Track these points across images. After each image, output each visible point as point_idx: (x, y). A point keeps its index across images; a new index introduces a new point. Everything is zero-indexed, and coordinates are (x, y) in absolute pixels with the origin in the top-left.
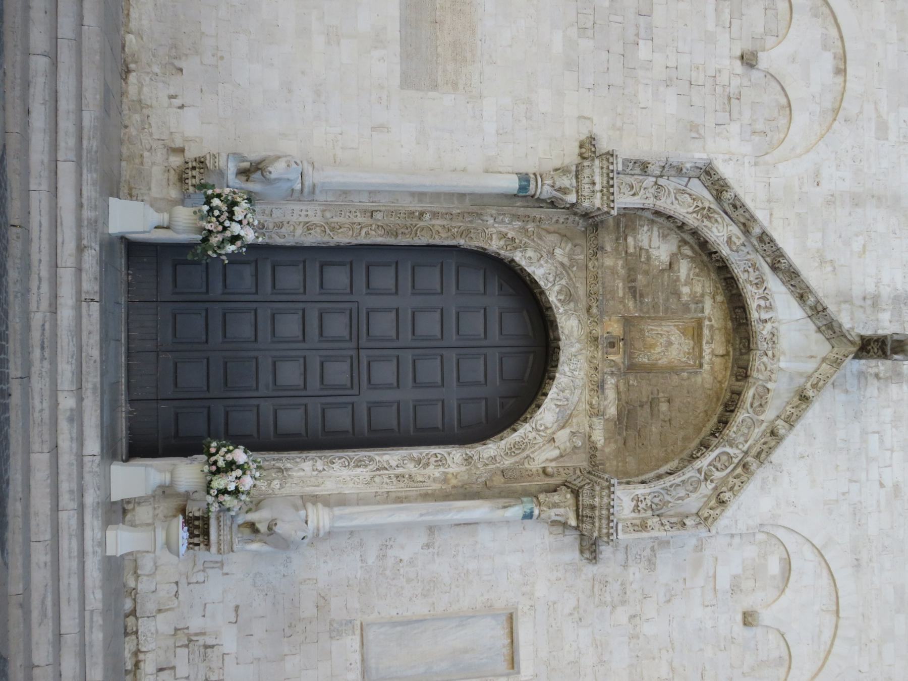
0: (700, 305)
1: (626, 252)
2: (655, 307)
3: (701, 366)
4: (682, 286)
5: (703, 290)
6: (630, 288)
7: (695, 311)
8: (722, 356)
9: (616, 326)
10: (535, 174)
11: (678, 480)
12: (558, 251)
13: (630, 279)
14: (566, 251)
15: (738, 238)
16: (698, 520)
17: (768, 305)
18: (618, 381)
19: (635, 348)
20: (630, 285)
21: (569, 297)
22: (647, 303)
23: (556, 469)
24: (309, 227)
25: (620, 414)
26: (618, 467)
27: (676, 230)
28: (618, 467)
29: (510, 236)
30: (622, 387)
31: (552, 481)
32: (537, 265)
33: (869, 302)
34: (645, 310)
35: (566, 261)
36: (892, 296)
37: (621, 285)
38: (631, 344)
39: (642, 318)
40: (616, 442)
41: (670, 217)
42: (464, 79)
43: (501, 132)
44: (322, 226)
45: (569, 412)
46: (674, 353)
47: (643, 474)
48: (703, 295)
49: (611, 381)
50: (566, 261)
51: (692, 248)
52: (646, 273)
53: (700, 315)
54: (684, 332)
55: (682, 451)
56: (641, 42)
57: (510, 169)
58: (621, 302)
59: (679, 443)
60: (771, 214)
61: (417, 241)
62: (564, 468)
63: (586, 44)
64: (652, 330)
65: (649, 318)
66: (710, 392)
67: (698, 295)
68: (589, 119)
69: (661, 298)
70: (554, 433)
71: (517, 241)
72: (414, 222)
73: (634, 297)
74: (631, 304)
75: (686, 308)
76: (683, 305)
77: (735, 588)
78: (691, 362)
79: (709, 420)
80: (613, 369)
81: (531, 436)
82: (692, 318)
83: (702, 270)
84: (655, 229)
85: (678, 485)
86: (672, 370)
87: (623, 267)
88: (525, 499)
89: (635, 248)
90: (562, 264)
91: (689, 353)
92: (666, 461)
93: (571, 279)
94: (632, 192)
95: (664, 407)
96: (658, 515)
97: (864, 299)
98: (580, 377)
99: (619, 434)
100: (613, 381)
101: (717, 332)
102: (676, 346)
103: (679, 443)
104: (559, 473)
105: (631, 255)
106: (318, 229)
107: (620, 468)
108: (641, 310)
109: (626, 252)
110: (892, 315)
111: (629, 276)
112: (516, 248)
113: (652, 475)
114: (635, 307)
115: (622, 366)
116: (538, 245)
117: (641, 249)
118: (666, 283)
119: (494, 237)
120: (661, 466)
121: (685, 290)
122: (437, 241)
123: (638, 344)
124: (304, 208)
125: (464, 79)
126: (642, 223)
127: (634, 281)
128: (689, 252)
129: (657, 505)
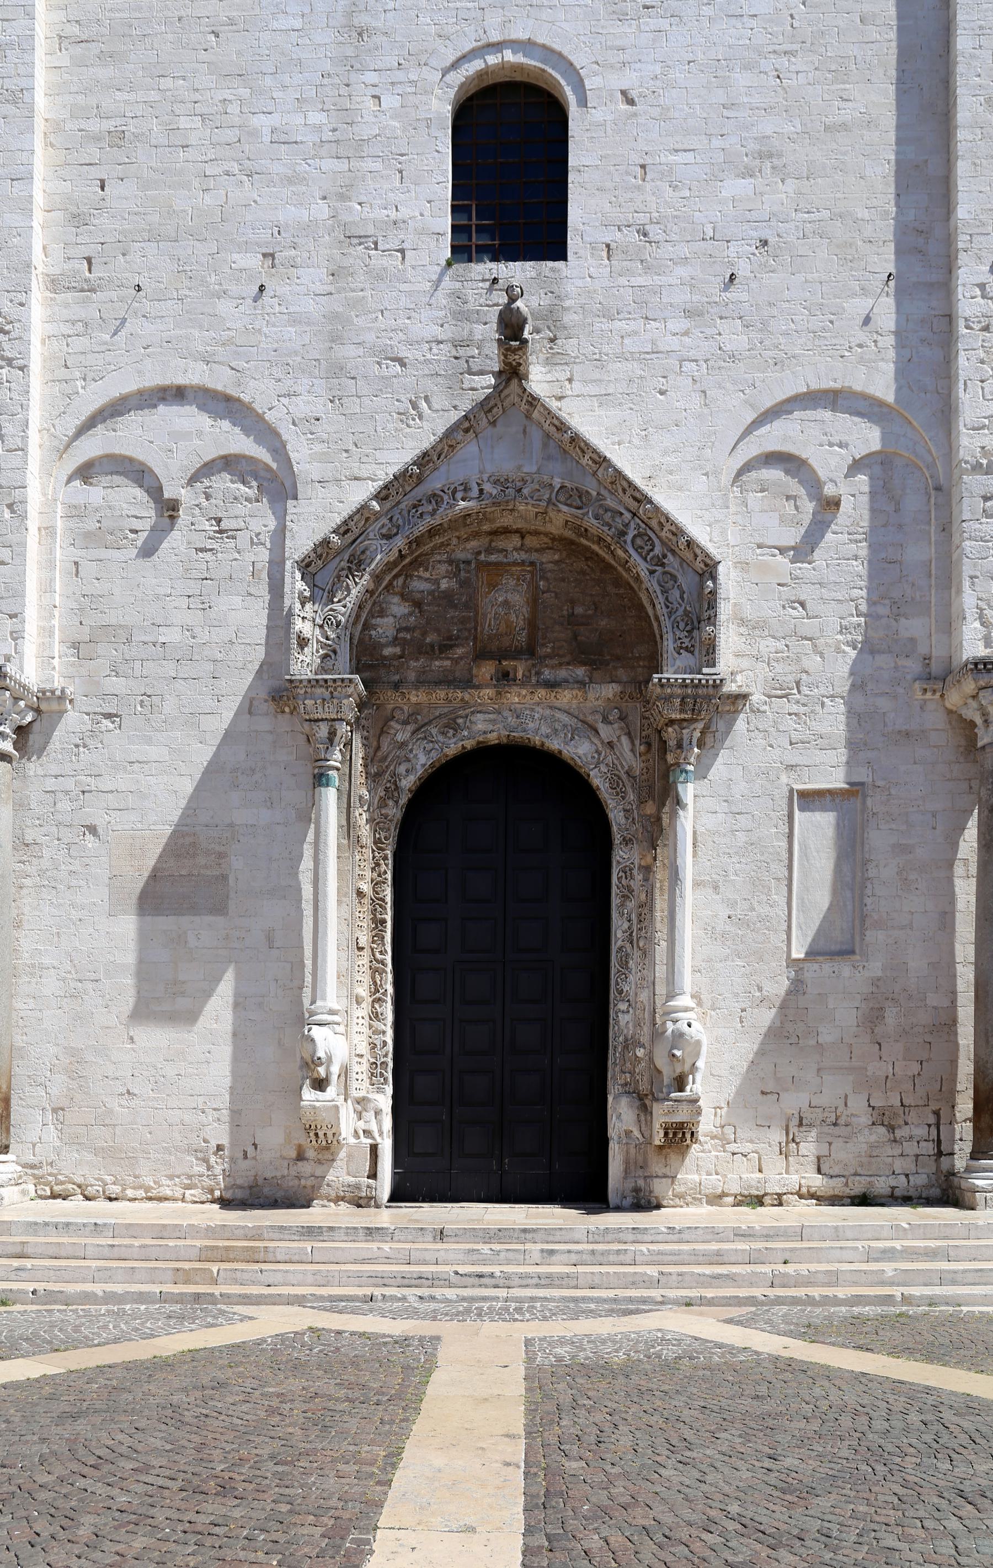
0: (462, 566)
1: (401, 657)
2: (463, 621)
3: (532, 564)
4: (439, 588)
5: (445, 562)
6: (441, 653)
7: (469, 572)
8: (523, 537)
9: (484, 670)
10: (314, 768)
11: (661, 599)
12: (400, 737)
13: (431, 651)
14: (399, 727)
15: (383, 526)
16: (707, 575)
17: (462, 488)
18: (547, 666)
19: (511, 646)
20: (437, 652)
21: (452, 725)
22: (458, 631)
23: (643, 740)
24: (376, 1016)
25: (583, 663)
26: (644, 667)
27: (375, 597)
28: (644, 667)
29: (383, 794)
30: (555, 661)
31: (655, 745)
32: (414, 761)
33: (461, 352)
34: (467, 634)
35: (410, 728)
36: (454, 323)
37: (437, 663)
38: (506, 650)
39: (475, 638)
40: (615, 668)
41: (360, 607)
42: (213, 846)
43: (269, 804)
44: (373, 1001)
45: (580, 725)
46: (517, 597)
47: (655, 636)
48: (450, 562)
49: (547, 674)
50: (410, 728)
51: (396, 577)
52: (424, 634)
53: (473, 566)
54: (493, 586)
55: (631, 588)
56: (162, 639)
57: (310, 793)
58: (457, 663)
59: (622, 591)
60: (356, 479)
61: (389, 899)
62: (642, 730)
63: (169, 706)
64: (489, 625)
65: (476, 629)
66: (564, 553)
67: (450, 568)
68: (251, 702)
69: (452, 614)
70: (602, 743)
71: (388, 785)
72: (366, 901)
73: (451, 647)
74: (460, 651)
75: (464, 583)
76: (461, 587)
77: (795, 521)
78: (528, 576)
79: (597, 555)
80: (533, 672)
81: (604, 769)
82: (477, 576)
83: (421, 565)
84: (373, 621)
85: (667, 599)
86: (534, 601)
87: (417, 660)
88: (671, 779)
89: (396, 646)
90: (413, 733)
91: (518, 579)
92: (641, 607)
93: (430, 722)
94: (333, 657)
95: (579, 610)
96: (699, 623)
97: (456, 358)
98: (541, 710)
99: (608, 664)
100: (547, 672)
101: (494, 544)
102: (509, 596)
103: (622, 591)
104: (648, 736)
105: (403, 650)
106: (377, 1006)
107: (646, 663)
108: (467, 639)
109: (401, 657)
110: (477, 322)
111: (427, 653)
112: (397, 788)
113: (655, 625)
114: (463, 646)
115: (530, 662)
116: (392, 761)
117: (396, 638)
118: (436, 609)
119: (383, 812)
120: (647, 613)
121: (444, 585)
122: (389, 876)
123: (506, 642)
124: (356, 1021)
125: (213, 846)
126: (367, 638)
127: (432, 646)
128: (400, 581)
129: (687, 625)
